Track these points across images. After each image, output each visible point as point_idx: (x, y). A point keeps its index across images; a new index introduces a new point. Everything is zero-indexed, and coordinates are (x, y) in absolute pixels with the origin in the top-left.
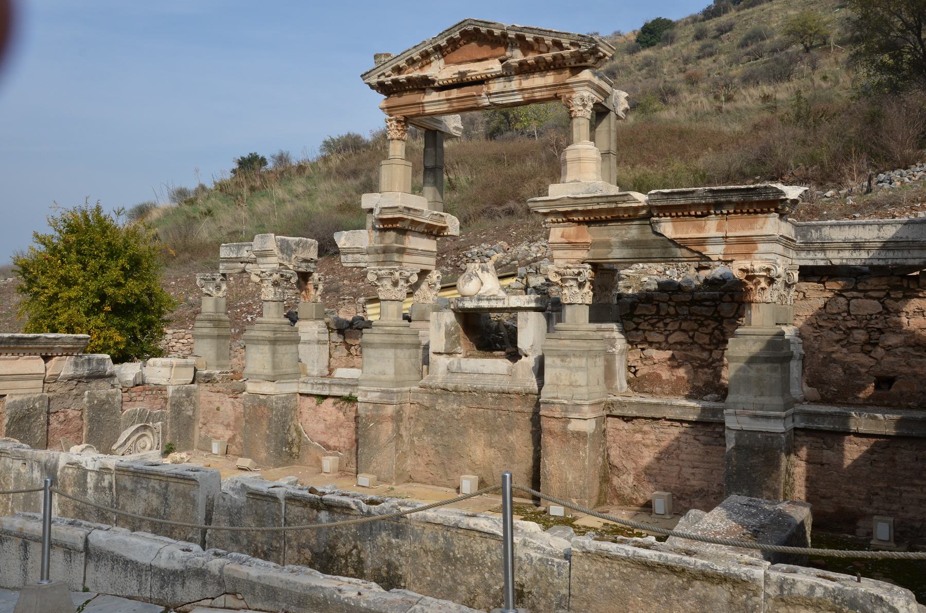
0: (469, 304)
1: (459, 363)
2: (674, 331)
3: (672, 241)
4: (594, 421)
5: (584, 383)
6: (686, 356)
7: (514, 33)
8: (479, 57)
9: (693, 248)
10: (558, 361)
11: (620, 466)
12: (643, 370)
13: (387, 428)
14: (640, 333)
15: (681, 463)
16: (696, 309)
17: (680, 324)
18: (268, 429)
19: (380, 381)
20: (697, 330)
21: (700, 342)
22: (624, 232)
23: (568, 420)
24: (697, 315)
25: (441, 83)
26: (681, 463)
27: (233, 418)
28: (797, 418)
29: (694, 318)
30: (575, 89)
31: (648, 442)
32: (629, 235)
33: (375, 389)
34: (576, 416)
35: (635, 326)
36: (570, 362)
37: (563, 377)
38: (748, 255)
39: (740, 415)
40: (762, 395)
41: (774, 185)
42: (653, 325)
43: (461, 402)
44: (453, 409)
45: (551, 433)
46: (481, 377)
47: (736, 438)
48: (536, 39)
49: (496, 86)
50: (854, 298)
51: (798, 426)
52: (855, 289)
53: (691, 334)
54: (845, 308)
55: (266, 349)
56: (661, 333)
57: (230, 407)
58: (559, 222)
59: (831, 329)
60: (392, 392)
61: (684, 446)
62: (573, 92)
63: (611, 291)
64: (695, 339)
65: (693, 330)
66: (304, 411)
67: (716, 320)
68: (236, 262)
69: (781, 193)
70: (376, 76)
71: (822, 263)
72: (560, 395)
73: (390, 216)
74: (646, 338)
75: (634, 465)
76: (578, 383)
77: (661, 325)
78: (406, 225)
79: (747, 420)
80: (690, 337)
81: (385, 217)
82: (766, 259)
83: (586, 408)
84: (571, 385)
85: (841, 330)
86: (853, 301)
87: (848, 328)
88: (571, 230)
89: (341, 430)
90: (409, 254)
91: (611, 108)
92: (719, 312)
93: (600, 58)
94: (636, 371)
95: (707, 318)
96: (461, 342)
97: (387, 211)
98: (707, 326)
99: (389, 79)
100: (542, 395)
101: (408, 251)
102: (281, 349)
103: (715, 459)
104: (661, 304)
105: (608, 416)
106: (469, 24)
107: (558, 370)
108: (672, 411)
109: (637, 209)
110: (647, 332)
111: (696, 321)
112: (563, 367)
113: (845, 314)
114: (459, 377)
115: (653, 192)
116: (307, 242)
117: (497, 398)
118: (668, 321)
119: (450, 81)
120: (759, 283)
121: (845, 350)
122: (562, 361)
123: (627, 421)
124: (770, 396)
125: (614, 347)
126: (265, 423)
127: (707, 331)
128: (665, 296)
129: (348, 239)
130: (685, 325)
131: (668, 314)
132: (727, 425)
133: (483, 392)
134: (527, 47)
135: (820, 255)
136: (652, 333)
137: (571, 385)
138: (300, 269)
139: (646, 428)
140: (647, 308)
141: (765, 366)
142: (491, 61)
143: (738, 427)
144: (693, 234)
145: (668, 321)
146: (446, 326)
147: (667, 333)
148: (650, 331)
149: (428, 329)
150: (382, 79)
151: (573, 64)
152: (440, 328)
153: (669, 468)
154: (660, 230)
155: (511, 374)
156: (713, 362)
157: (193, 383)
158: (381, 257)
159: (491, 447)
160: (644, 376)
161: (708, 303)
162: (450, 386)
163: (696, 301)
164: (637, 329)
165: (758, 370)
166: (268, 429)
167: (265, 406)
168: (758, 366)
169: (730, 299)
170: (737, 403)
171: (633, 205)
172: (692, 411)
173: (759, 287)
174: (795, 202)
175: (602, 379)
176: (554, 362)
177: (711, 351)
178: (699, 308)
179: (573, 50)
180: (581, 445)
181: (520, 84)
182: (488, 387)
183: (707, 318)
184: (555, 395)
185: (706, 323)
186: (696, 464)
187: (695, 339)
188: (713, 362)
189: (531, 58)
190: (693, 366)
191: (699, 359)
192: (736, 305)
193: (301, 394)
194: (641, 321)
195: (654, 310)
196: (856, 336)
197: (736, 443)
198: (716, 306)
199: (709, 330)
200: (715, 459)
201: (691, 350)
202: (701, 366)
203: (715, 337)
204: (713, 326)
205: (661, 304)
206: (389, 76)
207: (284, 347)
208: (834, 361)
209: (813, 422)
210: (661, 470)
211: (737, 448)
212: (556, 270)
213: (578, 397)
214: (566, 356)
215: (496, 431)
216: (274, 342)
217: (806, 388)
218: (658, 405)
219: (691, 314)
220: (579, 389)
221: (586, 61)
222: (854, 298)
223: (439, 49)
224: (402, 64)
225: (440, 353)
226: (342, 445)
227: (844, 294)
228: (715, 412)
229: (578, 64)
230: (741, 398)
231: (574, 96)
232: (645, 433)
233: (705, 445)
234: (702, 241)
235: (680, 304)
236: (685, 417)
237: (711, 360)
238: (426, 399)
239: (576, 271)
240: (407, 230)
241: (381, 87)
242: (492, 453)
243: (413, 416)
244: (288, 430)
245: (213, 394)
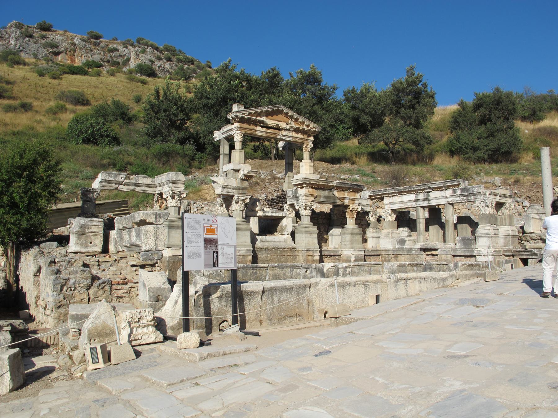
10: (309, 235)
49: (284, 133)
158: (241, 191)
182: (280, 247)
234: (344, 198)
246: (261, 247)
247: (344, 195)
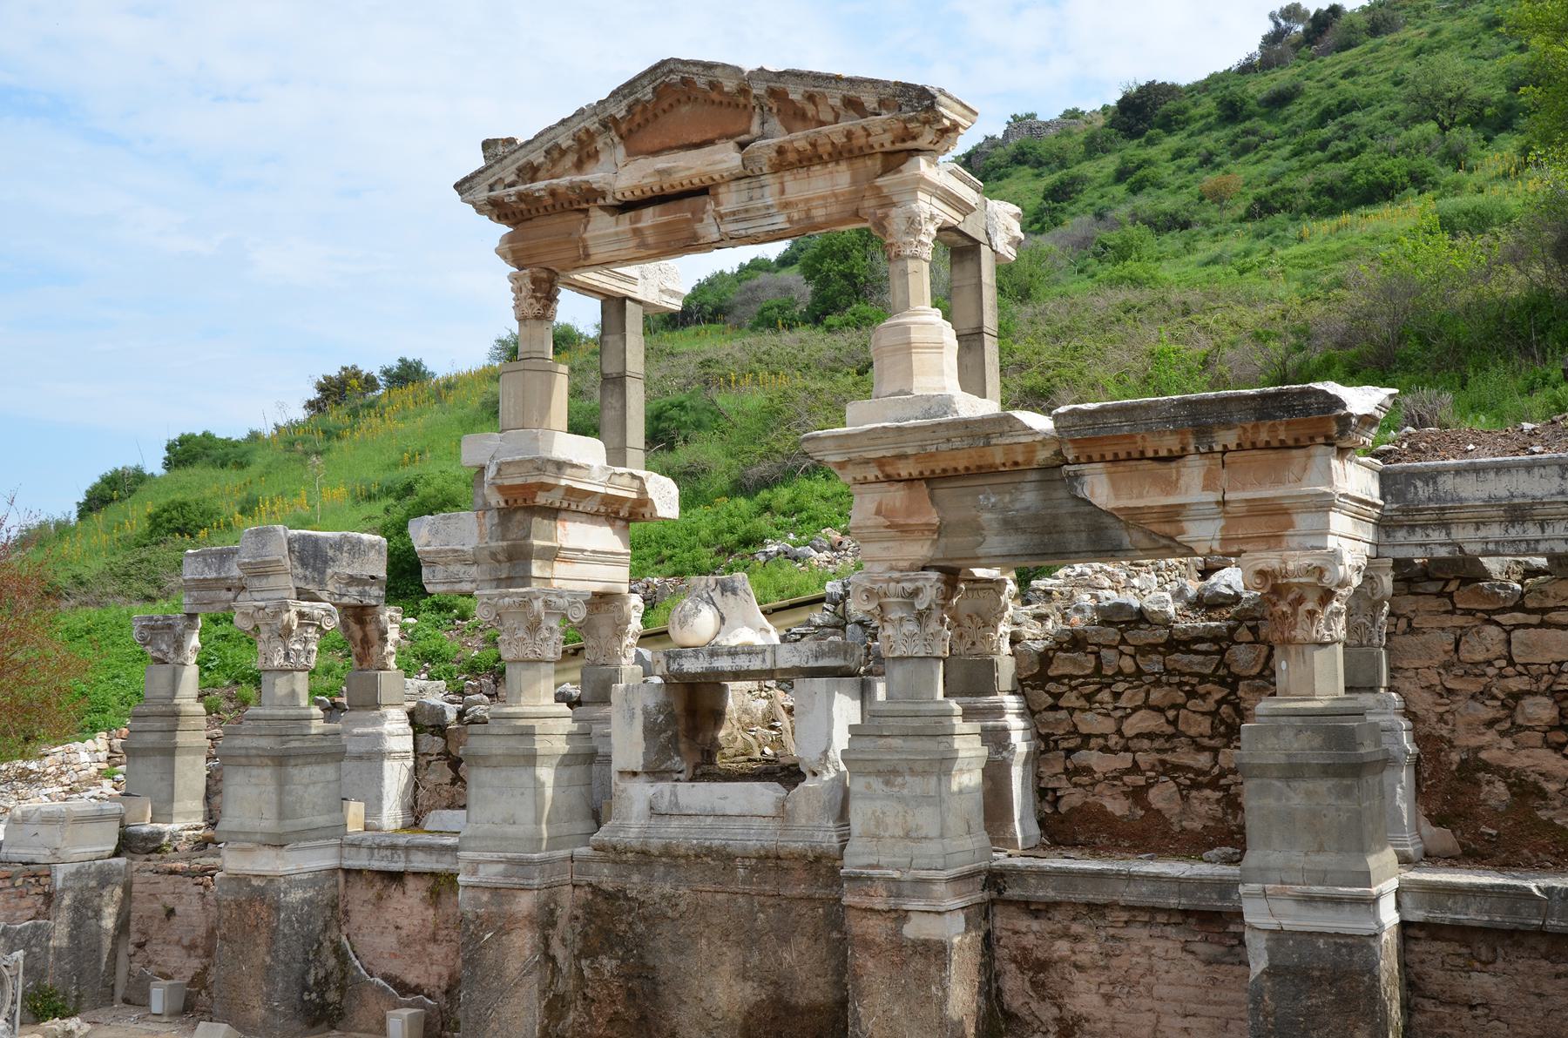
0: (692, 666)
1: (674, 794)
2: (1135, 709)
3: (1109, 514)
4: (961, 917)
5: (934, 832)
6: (1163, 762)
7: (764, 85)
8: (696, 139)
9: (1154, 528)
10: (877, 784)
11: (1023, 1012)
12: (1072, 798)
13: (523, 942)
14: (1062, 714)
15: (1157, 1005)
16: (1179, 659)
17: (1148, 693)
18: (269, 952)
19: (504, 838)
20: (1184, 706)
21: (1193, 732)
22: (1007, 498)
23: (902, 916)
24: (1182, 674)
25: (619, 196)
26: (1157, 1005)
27: (202, 931)
28: (1407, 900)
29: (1176, 679)
30: (895, 199)
31: (1082, 958)
32: (1018, 506)
34: (919, 905)
35: (1050, 700)
36: (903, 785)
37: (889, 820)
38: (1273, 540)
39: (1277, 896)
40: (1321, 849)
41: (1319, 386)
42: (1089, 698)
43: (679, 880)
44: (663, 897)
45: (867, 944)
46: (719, 822)
47: (1268, 949)
48: (811, 98)
50: (1517, 626)
51: (1410, 918)
52: (1519, 607)
53: (1171, 714)
54: (1500, 649)
55: (266, 774)
56: (1108, 715)
57: (197, 904)
58: (865, 482)
59: (1473, 697)
60: (531, 862)
61: (1162, 966)
62: (894, 205)
63: (995, 628)
64: (1182, 727)
65: (1174, 706)
66: (355, 907)
67: (1222, 682)
68: (220, 589)
69: (1338, 403)
70: (485, 186)
71: (1442, 552)
72: (883, 860)
73: (518, 481)
74: (1075, 726)
75: (1055, 1011)
76: (923, 833)
77: (1105, 696)
78: (554, 499)
79: (1291, 907)
80: (1168, 721)
81: (507, 482)
82: (1313, 548)
83: (939, 889)
84: (907, 836)
85: (1494, 698)
86: (1518, 634)
87: (1517, 696)
88: (896, 496)
89: (431, 948)
90: (566, 560)
91: (981, 237)
92: (1227, 666)
93: (944, 132)
94: (1059, 798)
95: (1203, 679)
96: (682, 747)
97: (511, 470)
98: (1203, 697)
99: (512, 190)
100: (846, 860)
101: (562, 554)
102: (302, 774)
103: (1232, 995)
104: (1104, 652)
105: (993, 902)
106: (671, 71)
107: (878, 804)
108: (1132, 888)
109: (1030, 448)
110: (1077, 714)
111: (1180, 685)
112: (889, 797)
113: (1503, 663)
114: (675, 823)
115: (1062, 410)
116: (360, 541)
117: (754, 870)
118: (1119, 687)
120: (1300, 600)
121: (1507, 743)
122: (887, 783)
123: (1036, 914)
124: (1339, 851)
125: (1006, 748)
126: (262, 939)
127: (1205, 708)
128: (1112, 634)
129: (435, 532)
130: (1156, 696)
131: (1120, 672)
132: (1247, 919)
133: (725, 857)
134: (794, 115)
135: (1437, 536)
136: (1089, 715)
137: (907, 836)
138: (345, 600)
139: (1077, 928)
140: (1075, 662)
142: (719, 146)
143: (1272, 923)
144: (1155, 499)
145: (1119, 687)
146: (646, 712)
147: (1119, 713)
148: (1083, 710)
149: (606, 720)
150: (499, 192)
151: (888, 147)
152: (632, 716)
153: (1131, 1017)
154: (1085, 492)
155: (783, 813)
156: (1222, 775)
157: (117, 854)
159: (745, 978)
160: (1073, 810)
161: (1203, 647)
162: (655, 844)
163: (1179, 642)
164: (1054, 708)
165: (1309, 794)
166: (269, 952)
167: (263, 900)
168: (1309, 785)
169: (1251, 638)
170: (1268, 869)
171: (1023, 439)
172: (1175, 887)
173: (1302, 609)
174: (1367, 421)
175: (978, 820)
176: (869, 786)
177: (1215, 751)
178: (1186, 658)
179: (885, 116)
180: (933, 970)
181: (782, 192)
182: (735, 846)
183: (1203, 679)
185: (1201, 689)
186: (1192, 1007)
187: (1182, 727)
188: (1222, 775)
189: (799, 139)
190: (1178, 785)
191: (1189, 768)
192: (1265, 649)
193: (348, 872)
194: (1065, 688)
195: (1091, 662)
196: (1529, 710)
197: (1270, 959)
198: (1222, 652)
199: (1209, 705)
200: (1232, 995)
201: (1173, 750)
202: (1196, 785)
203: (1222, 721)
204: (1218, 696)
205: (1104, 652)
206: (512, 185)
207: (307, 770)
208: (1486, 767)
209: (1441, 908)
210: (1114, 1022)
211: (1273, 972)
212: (868, 585)
213: (924, 862)
214: (895, 772)
215: (753, 942)
216: (281, 760)
217: (1428, 829)
218: (1099, 875)
219: (1169, 672)
220: (924, 844)
221: (914, 138)
222: (1517, 626)
223: (609, 124)
224: (538, 158)
225: (635, 774)
226: (434, 981)
227: (1497, 618)
228: (1226, 888)
229: (899, 146)
230: (1275, 858)
231: (894, 212)
232: (1077, 939)
233: (1209, 963)
234: (1173, 514)
235: (1144, 650)
236: (1160, 902)
237: (1216, 770)
238: (606, 876)
239: (909, 586)
240: (558, 510)
241: (497, 210)
242: (748, 991)
243: (579, 912)
244: (317, 952)
245: (161, 878)
246: (636, 844)
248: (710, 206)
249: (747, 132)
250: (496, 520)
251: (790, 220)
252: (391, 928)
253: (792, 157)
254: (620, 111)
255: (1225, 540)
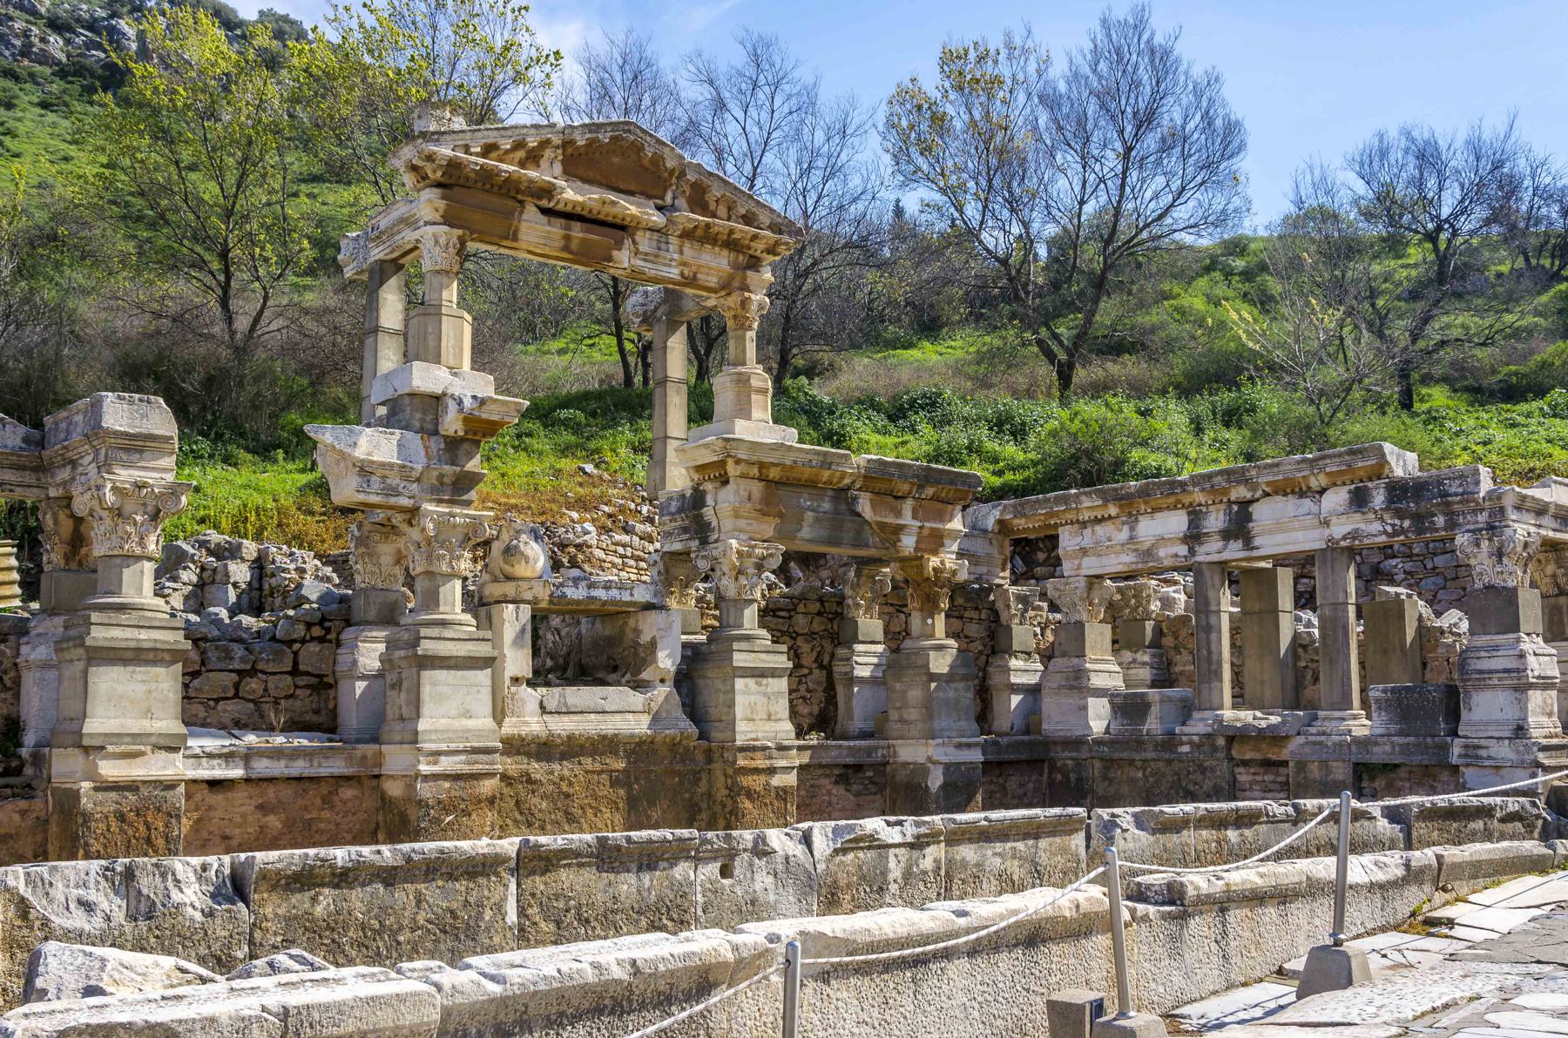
33: (461, 746)
37: (759, 708)
72: (760, 735)
79: (951, 750)
81: (484, 416)
119: (578, 209)
141: (961, 685)
143: (945, 760)
184: (753, 736)
198: (790, 618)
247: (898, 513)
248: (628, 242)
249: (662, 198)
250: (442, 446)
251: (682, 274)
252: (217, 840)
253: (699, 232)
254: (581, 143)
255: (916, 549)
